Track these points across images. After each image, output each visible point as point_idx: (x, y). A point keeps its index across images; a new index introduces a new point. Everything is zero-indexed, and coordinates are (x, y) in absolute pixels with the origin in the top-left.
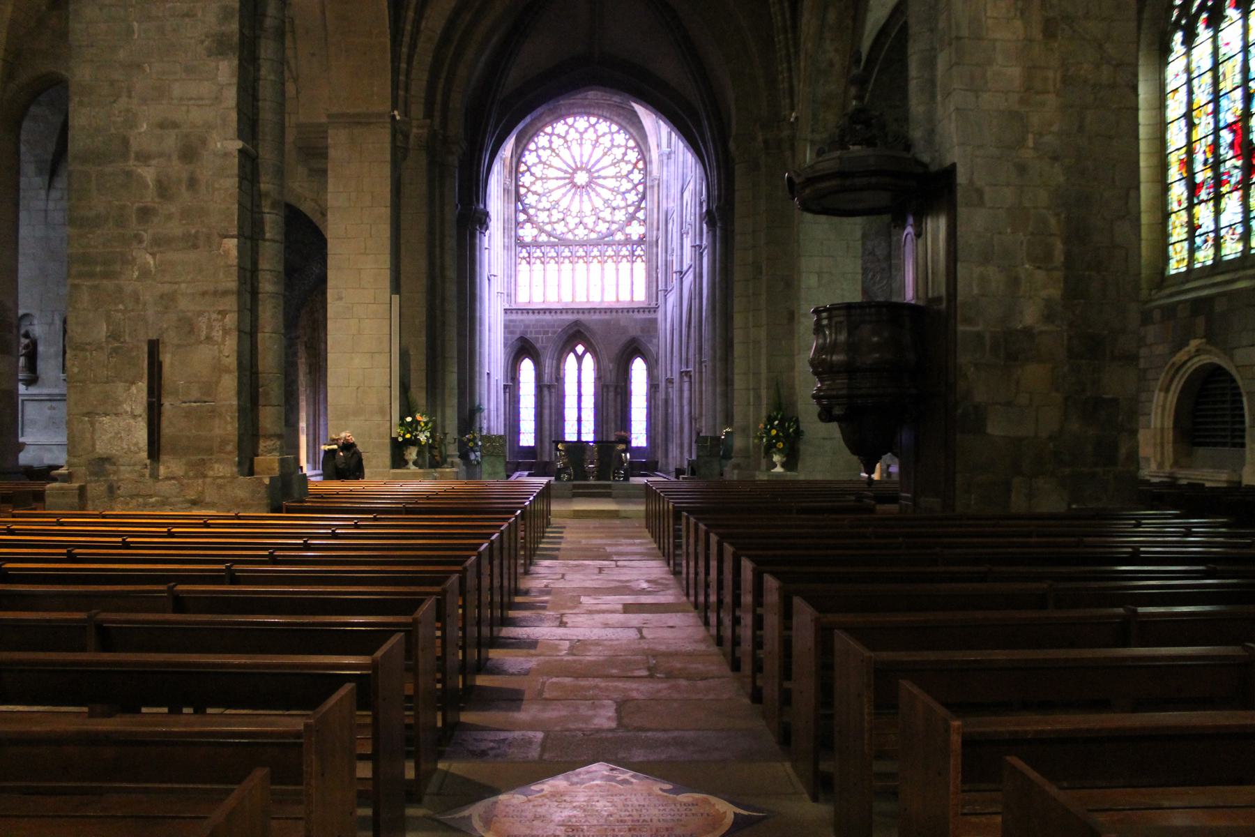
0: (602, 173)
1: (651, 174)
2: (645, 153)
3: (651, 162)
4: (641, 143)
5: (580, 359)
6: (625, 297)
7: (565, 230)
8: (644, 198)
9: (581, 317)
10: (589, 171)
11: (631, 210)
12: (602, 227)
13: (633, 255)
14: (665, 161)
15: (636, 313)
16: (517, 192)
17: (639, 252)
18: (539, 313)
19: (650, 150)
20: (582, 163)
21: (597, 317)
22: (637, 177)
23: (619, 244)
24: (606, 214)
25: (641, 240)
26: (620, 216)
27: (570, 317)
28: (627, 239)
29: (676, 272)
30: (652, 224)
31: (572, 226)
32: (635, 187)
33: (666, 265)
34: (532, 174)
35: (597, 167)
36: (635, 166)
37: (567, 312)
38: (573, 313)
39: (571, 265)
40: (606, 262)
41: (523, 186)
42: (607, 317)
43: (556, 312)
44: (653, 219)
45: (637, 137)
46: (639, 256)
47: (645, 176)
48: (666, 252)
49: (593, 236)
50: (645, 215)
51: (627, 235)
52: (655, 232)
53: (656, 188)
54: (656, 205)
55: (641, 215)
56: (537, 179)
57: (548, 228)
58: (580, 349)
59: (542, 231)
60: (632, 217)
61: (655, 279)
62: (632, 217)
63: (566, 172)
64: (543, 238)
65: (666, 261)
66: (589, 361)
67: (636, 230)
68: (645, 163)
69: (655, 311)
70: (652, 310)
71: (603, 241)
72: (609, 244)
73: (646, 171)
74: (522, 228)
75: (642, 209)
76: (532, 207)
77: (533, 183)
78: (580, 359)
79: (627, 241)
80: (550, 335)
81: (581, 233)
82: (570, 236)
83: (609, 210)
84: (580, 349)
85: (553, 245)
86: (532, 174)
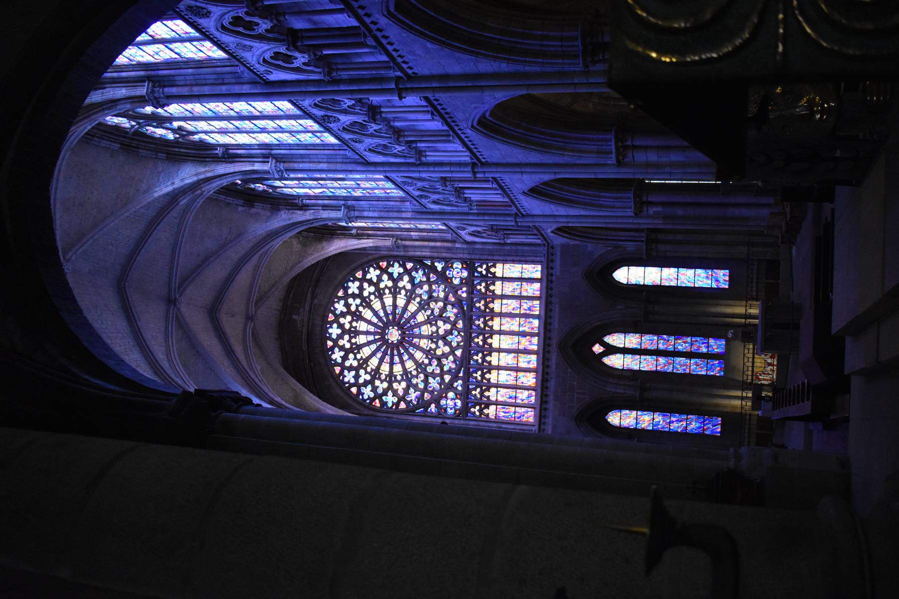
0: (389, 309)
1: (388, 249)
2: (370, 257)
3: (377, 248)
4: (359, 263)
5: (611, 350)
6: (534, 289)
7: (451, 358)
8: (419, 262)
9: (554, 342)
10: (387, 325)
11: (433, 277)
12: (451, 312)
13: (486, 276)
14: (357, 214)
15: (553, 271)
16: (403, 412)
17: (483, 270)
18: (546, 395)
19: (364, 249)
20: (374, 334)
21: (556, 324)
22: (396, 270)
23: (472, 293)
24: (437, 307)
25: (470, 266)
26: (440, 292)
27: (554, 357)
28: (466, 283)
29: (474, 173)
30: (448, 249)
31: (447, 349)
32: (408, 272)
33: (484, 214)
34: (385, 393)
35: (382, 314)
36: (384, 271)
37: (548, 359)
38: (549, 352)
39: (493, 354)
40: (492, 310)
41: (398, 404)
42: (556, 309)
43: (547, 374)
44: (441, 247)
45: (355, 265)
46: (487, 269)
47: (397, 258)
48: (467, 214)
49: (460, 324)
50: (440, 259)
51: (461, 283)
52: (457, 245)
53: (407, 243)
54: (426, 243)
55: (439, 266)
56: (390, 387)
57: (447, 378)
58: (597, 349)
59: (450, 387)
60: (443, 277)
61: (513, 247)
62: (443, 277)
63: (385, 354)
64: (459, 384)
65: (478, 214)
66: (615, 340)
67: (458, 273)
68: (382, 258)
69: (552, 248)
70: (551, 250)
71: (467, 312)
72: (471, 305)
73: (391, 259)
74: (445, 410)
75: (433, 263)
76: (423, 395)
77: (395, 393)
78: (611, 350)
79: (469, 283)
80: (575, 383)
81: (455, 339)
82: (459, 353)
83: (432, 305)
84: (597, 349)
85: (468, 375)
86: (385, 393)
